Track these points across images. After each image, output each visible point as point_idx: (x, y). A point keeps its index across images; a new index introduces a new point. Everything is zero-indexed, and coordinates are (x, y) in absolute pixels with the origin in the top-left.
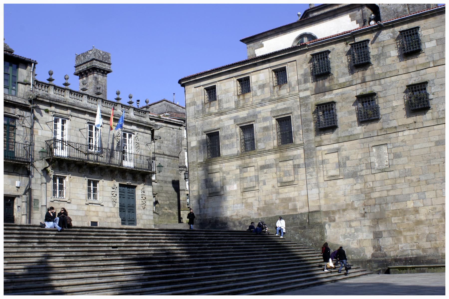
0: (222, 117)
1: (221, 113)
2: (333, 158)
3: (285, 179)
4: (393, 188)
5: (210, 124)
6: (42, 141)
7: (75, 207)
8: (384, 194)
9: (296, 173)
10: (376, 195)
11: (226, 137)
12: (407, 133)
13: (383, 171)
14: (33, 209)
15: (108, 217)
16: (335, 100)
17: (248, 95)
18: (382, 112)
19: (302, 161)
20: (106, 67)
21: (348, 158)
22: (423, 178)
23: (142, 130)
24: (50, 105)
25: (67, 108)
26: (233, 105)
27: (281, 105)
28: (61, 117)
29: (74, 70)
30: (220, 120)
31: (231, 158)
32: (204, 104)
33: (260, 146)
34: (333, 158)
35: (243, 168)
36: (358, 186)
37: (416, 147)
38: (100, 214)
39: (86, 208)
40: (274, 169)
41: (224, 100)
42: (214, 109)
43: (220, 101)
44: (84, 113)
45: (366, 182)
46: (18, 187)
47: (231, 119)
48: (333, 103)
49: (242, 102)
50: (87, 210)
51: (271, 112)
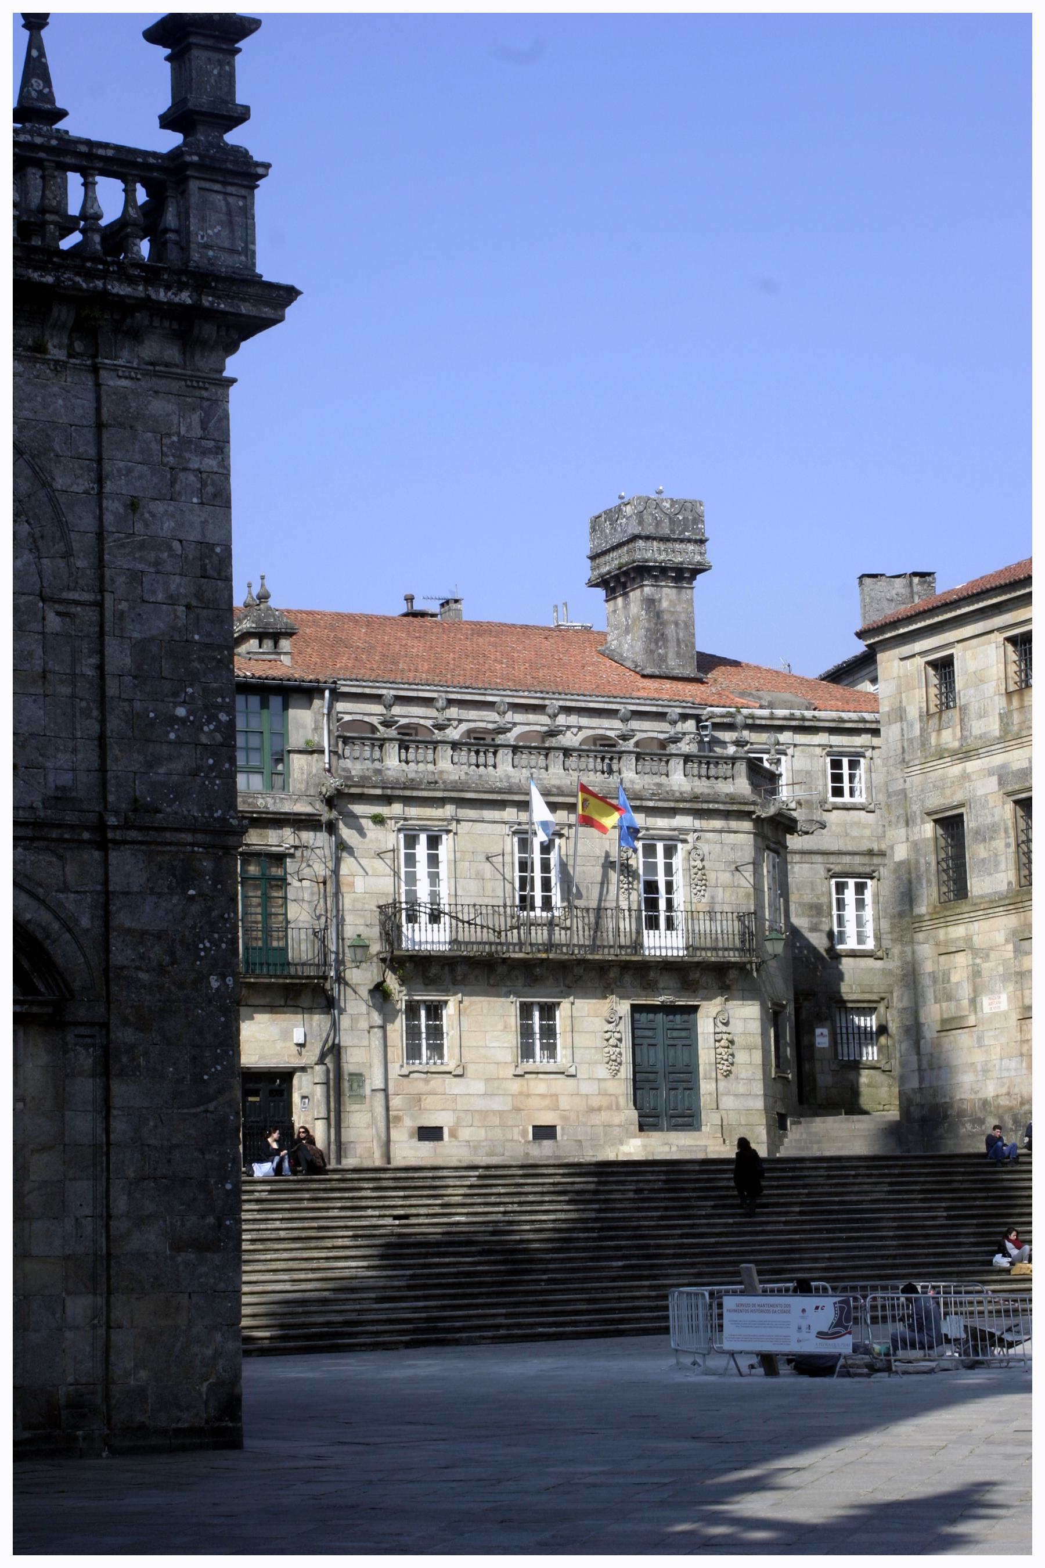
0: (972, 766)
1: (965, 754)
5: (940, 787)
6: (367, 907)
7: (479, 1087)
11: (981, 836)
14: (346, 1099)
15: (592, 1110)
20: (683, 555)
23: (718, 824)
24: (388, 800)
25: (442, 802)
26: (994, 727)
28: (423, 829)
29: (585, 571)
30: (965, 777)
32: (927, 715)
38: (564, 1103)
39: (516, 1086)
41: (974, 708)
42: (949, 738)
43: (964, 709)
44: (502, 805)
46: (301, 1046)
47: (990, 773)
49: (1016, 718)
50: (521, 1094)
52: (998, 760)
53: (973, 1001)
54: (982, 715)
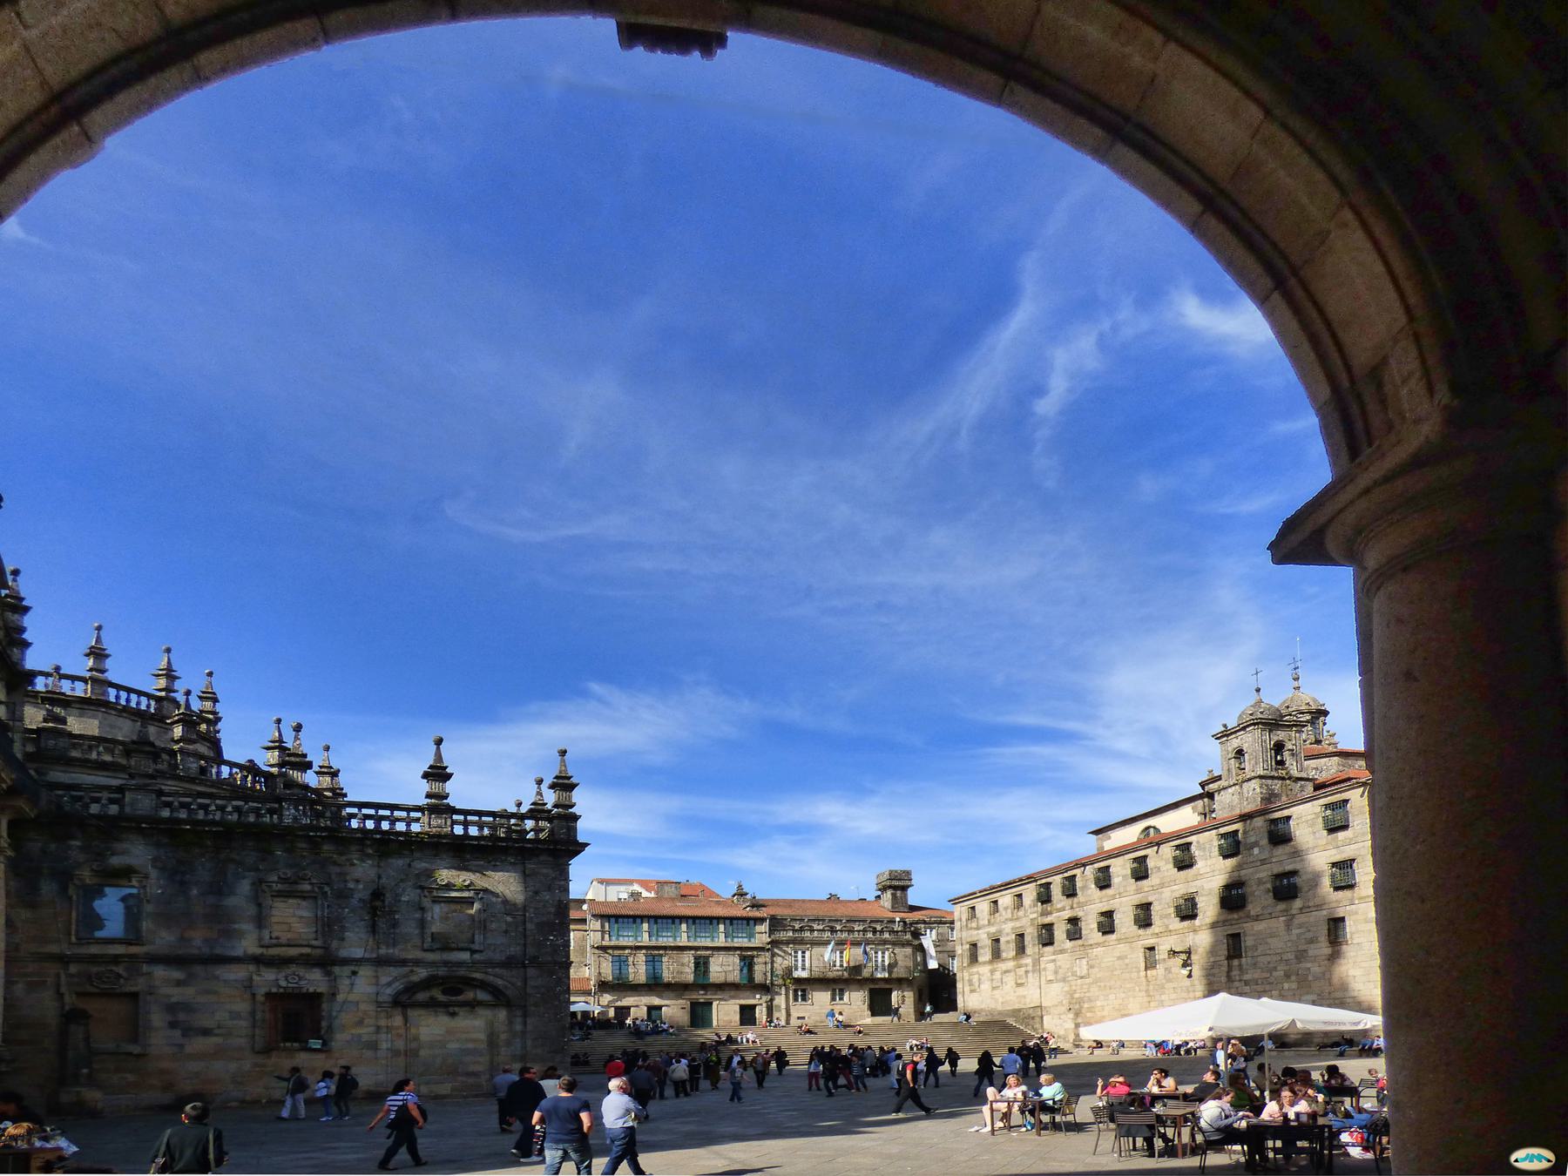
0: (980, 931)
1: (978, 928)
2: (1051, 966)
3: (1019, 982)
4: (1089, 991)
5: (971, 936)
8: (1082, 995)
9: (1027, 977)
10: (1077, 996)
11: (981, 947)
12: (1099, 949)
13: (1082, 978)
16: (1054, 921)
17: (997, 915)
18: (1083, 932)
19: (1030, 968)
21: (1060, 967)
22: (1108, 984)
26: (986, 922)
27: (1018, 924)
30: (978, 934)
31: (984, 963)
33: (1004, 955)
34: (1051, 966)
35: (992, 972)
36: (1066, 989)
37: (1105, 960)
40: (1012, 974)
41: (981, 918)
42: (974, 925)
45: (1071, 986)
48: (1052, 924)
51: (1012, 929)
52: (987, 930)
53: (979, 986)
54: (983, 919)
